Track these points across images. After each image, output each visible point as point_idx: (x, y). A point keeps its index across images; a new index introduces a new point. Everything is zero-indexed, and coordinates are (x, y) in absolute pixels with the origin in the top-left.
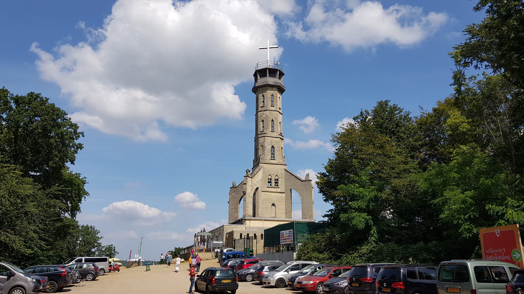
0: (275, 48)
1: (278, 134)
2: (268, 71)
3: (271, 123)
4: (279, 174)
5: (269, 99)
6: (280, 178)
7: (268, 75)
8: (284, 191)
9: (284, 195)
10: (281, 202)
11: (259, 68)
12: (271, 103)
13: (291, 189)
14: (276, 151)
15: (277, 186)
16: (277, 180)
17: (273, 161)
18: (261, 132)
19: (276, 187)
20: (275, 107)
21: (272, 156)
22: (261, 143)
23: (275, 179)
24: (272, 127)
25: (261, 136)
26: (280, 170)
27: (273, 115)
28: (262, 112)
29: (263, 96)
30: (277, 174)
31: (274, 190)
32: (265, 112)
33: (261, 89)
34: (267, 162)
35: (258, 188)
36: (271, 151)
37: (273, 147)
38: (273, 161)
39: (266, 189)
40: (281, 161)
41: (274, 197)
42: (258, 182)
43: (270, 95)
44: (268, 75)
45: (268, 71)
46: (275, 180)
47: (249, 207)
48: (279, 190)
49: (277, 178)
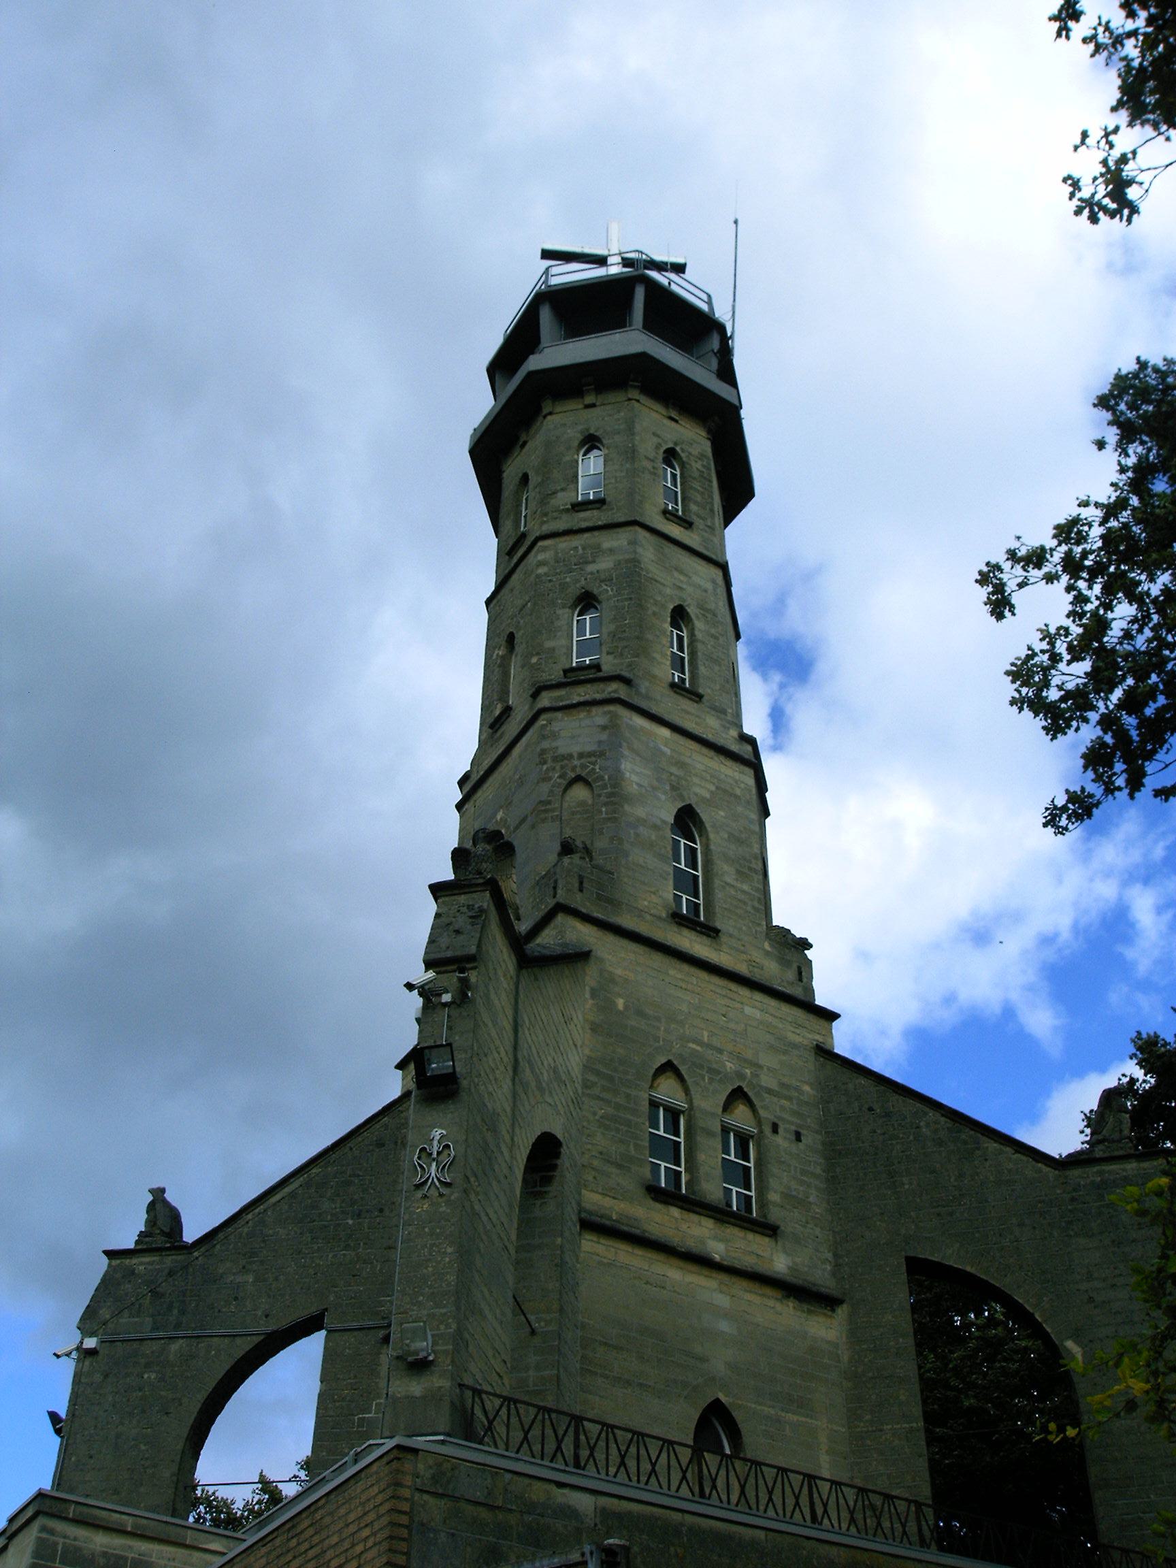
8: (822, 1276)
14: (726, 867)
22: (570, 756)
41: (724, 1326)
48: (780, 1263)
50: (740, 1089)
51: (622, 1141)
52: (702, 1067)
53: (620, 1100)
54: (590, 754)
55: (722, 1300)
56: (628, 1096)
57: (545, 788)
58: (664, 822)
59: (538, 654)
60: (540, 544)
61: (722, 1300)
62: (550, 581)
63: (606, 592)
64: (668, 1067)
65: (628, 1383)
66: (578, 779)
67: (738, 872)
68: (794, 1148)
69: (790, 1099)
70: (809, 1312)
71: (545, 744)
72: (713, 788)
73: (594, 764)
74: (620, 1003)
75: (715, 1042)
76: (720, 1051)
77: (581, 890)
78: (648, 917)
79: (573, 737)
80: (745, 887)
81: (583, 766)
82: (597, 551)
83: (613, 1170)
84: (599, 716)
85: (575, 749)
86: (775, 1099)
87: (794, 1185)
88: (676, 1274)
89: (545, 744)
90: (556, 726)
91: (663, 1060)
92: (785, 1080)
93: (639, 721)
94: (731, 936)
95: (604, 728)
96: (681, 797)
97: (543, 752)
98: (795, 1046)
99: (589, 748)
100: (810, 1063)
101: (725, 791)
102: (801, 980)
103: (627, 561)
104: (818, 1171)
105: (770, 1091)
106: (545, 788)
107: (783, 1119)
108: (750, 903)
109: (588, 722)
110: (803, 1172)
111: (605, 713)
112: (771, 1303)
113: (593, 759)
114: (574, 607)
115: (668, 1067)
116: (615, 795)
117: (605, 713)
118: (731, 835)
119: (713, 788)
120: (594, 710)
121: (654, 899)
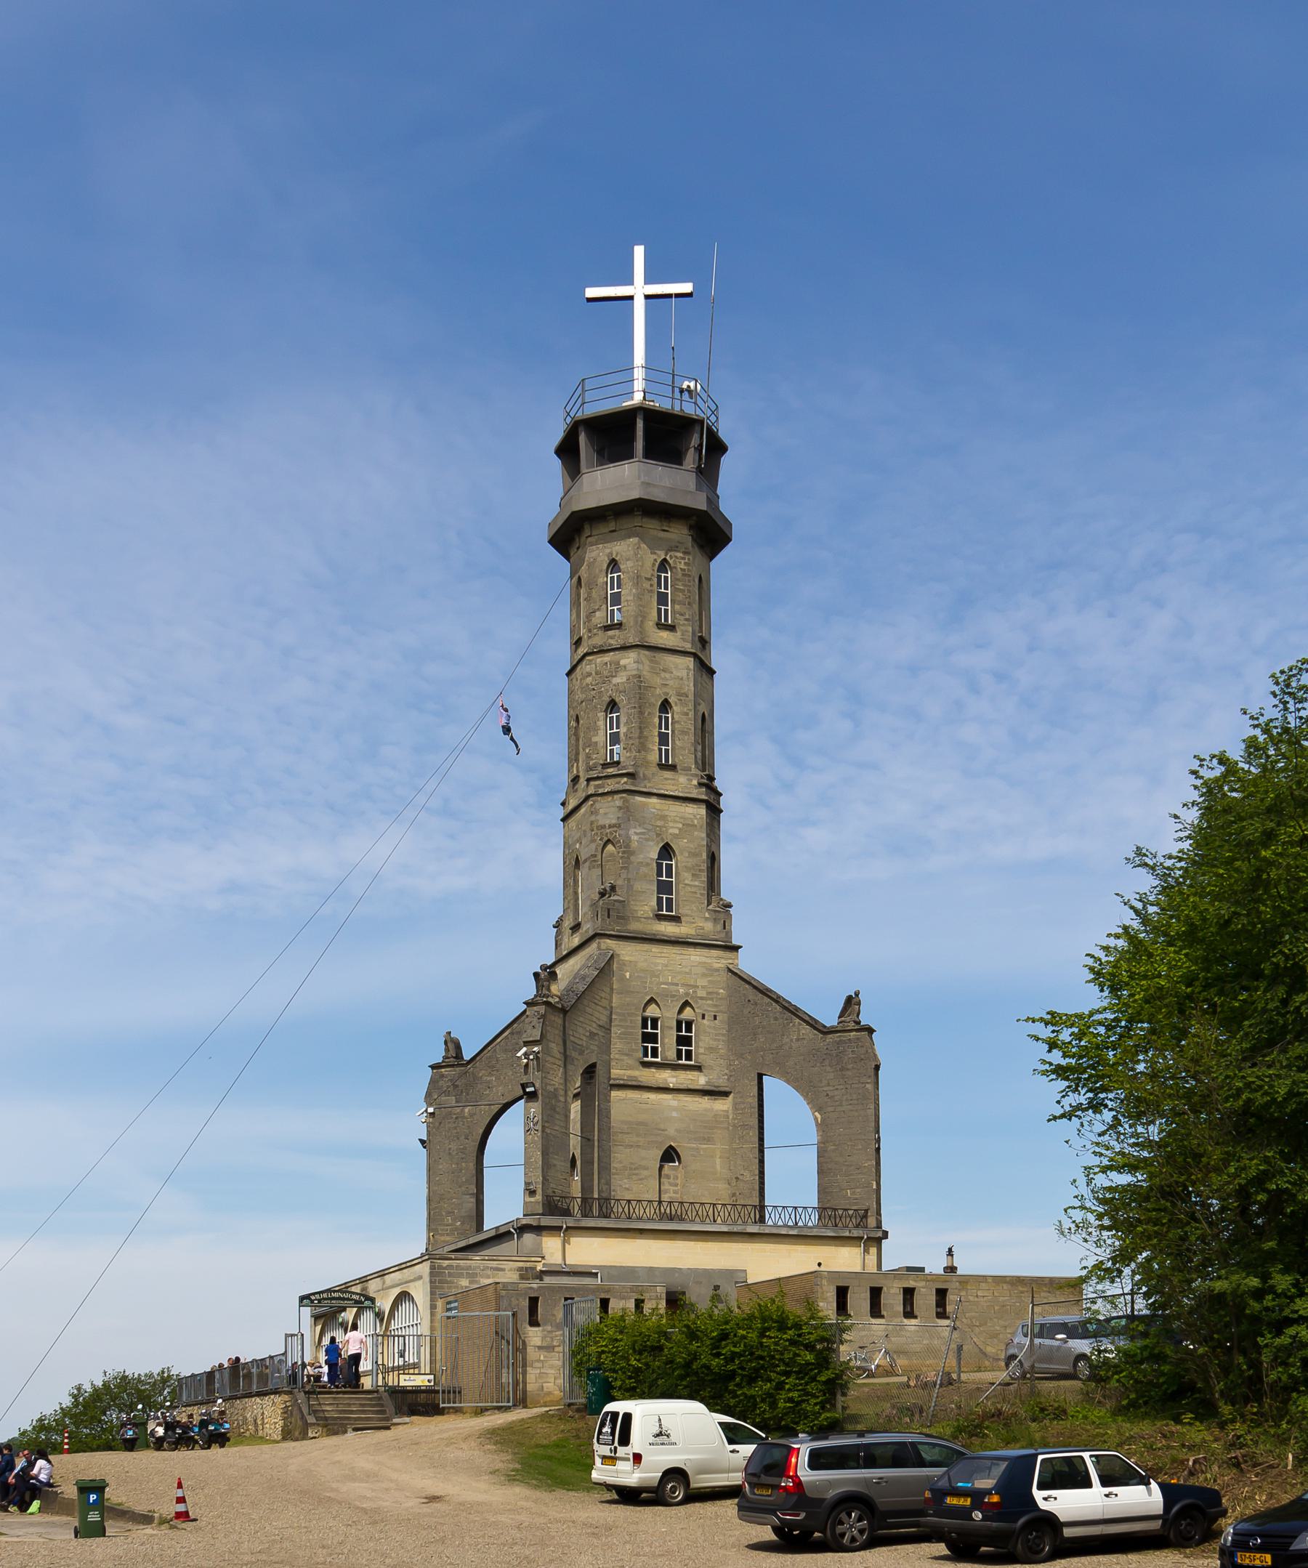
0: (678, 295)
1: (695, 782)
2: (640, 424)
3: (656, 720)
4: (701, 993)
5: (646, 585)
6: (703, 1017)
7: (639, 445)
8: (722, 1083)
9: (722, 1105)
10: (709, 1140)
11: (591, 410)
12: (659, 610)
13: (760, 1076)
14: (686, 874)
15: (689, 1057)
16: (689, 1025)
17: (668, 929)
18: (605, 766)
19: (683, 1062)
20: (679, 633)
21: (660, 900)
22: (603, 827)
23: (679, 1023)
24: (663, 739)
25: (601, 791)
26: (704, 975)
27: (667, 675)
28: (607, 658)
29: (613, 565)
30: (687, 994)
31: (674, 1080)
32: (628, 659)
33: (603, 529)
34: (635, 926)
35: (593, 1066)
36: (659, 874)
37: (667, 851)
38: (668, 929)
39: (629, 1073)
40: (709, 926)
41: (674, 1114)
42: (592, 1035)
43: (654, 565)
44: (639, 445)
45: (640, 424)
46: (679, 1029)
47: (555, 1165)
48: (701, 1080)
49: (688, 1014)
50: (687, 1001)
51: (629, 1043)
52: (667, 996)
53: (628, 1024)
54: (614, 826)
55: (674, 1103)
56: (631, 1021)
57: (593, 846)
58: (652, 859)
59: (589, 746)
60: (588, 658)
61: (674, 1103)
62: (594, 689)
63: (621, 699)
64: (652, 1000)
65: (632, 1146)
66: (609, 841)
67: (693, 875)
68: (712, 1024)
69: (712, 999)
70: (715, 1099)
71: (593, 818)
72: (680, 826)
73: (616, 832)
74: (628, 975)
75: (675, 981)
76: (677, 985)
77: (609, 917)
78: (643, 920)
79: (605, 814)
80: (697, 883)
81: (611, 833)
82: (618, 667)
83: (626, 1058)
84: (617, 801)
85: (607, 822)
86: (704, 1002)
87: (711, 1042)
88: (652, 1096)
89: (593, 818)
90: (597, 805)
91: (648, 998)
92: (710, 990)
93: (639, 799)
94: (687, 915)
95: (620, 808)
96: (662, 839)
97: (592, 823)
98: (717, 970)
99: (614, 821)
100: (725, 976)
101: (688, 825)
102: (725, 928)
103: (634, 676)
104: (725, 1032)
105: (702, 998)
106: (593, 846)
107: (708, 1011)
108: (698, 892)
109: (612, 804)
110: (716, 1035)
111: (621, 798)
112: (697, 1099)
113: (615, 829)
114: (606, 711)
115: (652, 1000)
116: (628, 852)
117: (621, 798)
118: (690, 853)
119: (680, 826)
120: (616, 797)
121: (646, 908)
